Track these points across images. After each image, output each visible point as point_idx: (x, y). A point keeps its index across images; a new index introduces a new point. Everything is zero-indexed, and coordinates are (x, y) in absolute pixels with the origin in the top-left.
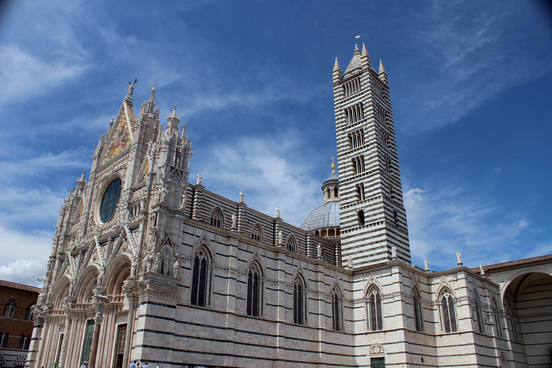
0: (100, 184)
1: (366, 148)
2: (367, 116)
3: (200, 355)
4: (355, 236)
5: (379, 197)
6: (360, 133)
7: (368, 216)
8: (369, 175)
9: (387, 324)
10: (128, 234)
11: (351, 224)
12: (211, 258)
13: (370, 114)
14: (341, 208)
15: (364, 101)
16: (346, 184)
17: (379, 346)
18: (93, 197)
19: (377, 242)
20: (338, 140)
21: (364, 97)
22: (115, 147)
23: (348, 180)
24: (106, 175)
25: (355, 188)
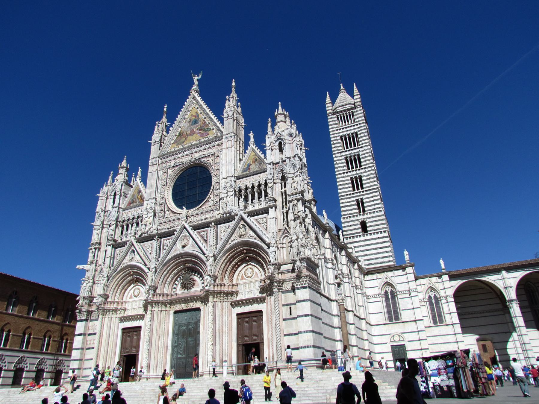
0: (170, 172)
1: (364, 170)
2: (363, 144)
3: (329, 340)
4: (359, 242)
5: (381, 211)
6: (357, 157)
7: (371, 226)
8: (368, 192)
9: (405, 316)
10: (248, 219)
11: (354, 232)
12: (320, 249)
13: (366, 143)
14: (344, 218)
15: (360, 131)
16: (347, 198)
17: (399, 335)
18: (160, 182)
19: (381, 248)
20: (336, 161)
21: (359, 128)
22: (189, 135)
23: (347, 195)
24: (178, 161)
25: (355, 202)
